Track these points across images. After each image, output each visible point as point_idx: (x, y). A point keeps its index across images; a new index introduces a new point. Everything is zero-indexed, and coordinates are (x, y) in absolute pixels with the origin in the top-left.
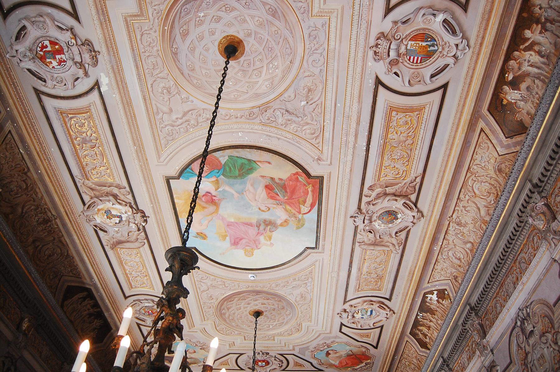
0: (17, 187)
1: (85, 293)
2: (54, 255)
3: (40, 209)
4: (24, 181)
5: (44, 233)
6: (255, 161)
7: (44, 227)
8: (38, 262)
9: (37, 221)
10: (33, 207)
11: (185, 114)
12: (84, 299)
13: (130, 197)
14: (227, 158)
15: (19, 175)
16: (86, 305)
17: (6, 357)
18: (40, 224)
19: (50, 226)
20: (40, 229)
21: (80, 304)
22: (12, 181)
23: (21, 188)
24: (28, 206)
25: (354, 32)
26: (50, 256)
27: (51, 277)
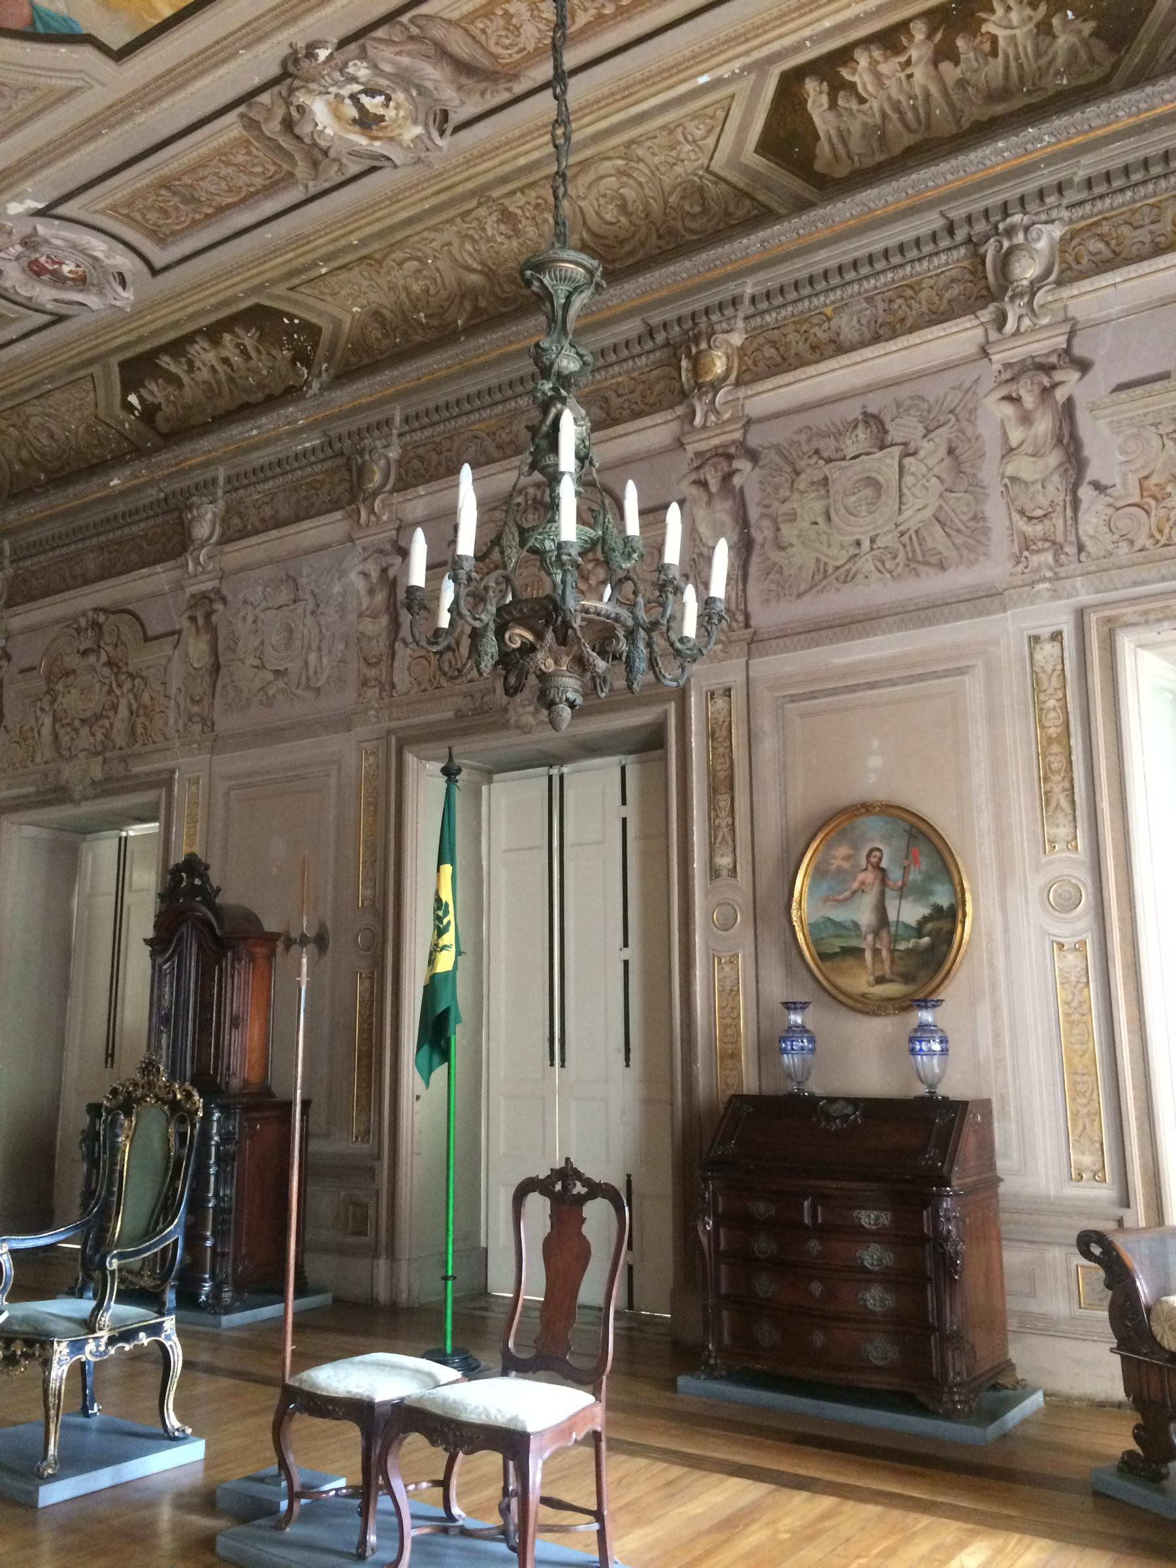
0: (416, 280)
1: (811, 85)
2: (622, 197)
3: (471, 232)
4: (400, 265)
5: (545, 221)
7: (524, 222)
8: (627, 248)
9: (508, 237)
10: (469, 247)
12: (838, 87)
13: (265, 98)
15: (388, 273)
16: (878, 76)
17: (698, 468)
18: (517, 232)
20: (532, 232)
21: (862, 101)
22: (406, 288)
23: (419, 271)
24: (467, 258)
26: (623, 208)
27: (697, 209)
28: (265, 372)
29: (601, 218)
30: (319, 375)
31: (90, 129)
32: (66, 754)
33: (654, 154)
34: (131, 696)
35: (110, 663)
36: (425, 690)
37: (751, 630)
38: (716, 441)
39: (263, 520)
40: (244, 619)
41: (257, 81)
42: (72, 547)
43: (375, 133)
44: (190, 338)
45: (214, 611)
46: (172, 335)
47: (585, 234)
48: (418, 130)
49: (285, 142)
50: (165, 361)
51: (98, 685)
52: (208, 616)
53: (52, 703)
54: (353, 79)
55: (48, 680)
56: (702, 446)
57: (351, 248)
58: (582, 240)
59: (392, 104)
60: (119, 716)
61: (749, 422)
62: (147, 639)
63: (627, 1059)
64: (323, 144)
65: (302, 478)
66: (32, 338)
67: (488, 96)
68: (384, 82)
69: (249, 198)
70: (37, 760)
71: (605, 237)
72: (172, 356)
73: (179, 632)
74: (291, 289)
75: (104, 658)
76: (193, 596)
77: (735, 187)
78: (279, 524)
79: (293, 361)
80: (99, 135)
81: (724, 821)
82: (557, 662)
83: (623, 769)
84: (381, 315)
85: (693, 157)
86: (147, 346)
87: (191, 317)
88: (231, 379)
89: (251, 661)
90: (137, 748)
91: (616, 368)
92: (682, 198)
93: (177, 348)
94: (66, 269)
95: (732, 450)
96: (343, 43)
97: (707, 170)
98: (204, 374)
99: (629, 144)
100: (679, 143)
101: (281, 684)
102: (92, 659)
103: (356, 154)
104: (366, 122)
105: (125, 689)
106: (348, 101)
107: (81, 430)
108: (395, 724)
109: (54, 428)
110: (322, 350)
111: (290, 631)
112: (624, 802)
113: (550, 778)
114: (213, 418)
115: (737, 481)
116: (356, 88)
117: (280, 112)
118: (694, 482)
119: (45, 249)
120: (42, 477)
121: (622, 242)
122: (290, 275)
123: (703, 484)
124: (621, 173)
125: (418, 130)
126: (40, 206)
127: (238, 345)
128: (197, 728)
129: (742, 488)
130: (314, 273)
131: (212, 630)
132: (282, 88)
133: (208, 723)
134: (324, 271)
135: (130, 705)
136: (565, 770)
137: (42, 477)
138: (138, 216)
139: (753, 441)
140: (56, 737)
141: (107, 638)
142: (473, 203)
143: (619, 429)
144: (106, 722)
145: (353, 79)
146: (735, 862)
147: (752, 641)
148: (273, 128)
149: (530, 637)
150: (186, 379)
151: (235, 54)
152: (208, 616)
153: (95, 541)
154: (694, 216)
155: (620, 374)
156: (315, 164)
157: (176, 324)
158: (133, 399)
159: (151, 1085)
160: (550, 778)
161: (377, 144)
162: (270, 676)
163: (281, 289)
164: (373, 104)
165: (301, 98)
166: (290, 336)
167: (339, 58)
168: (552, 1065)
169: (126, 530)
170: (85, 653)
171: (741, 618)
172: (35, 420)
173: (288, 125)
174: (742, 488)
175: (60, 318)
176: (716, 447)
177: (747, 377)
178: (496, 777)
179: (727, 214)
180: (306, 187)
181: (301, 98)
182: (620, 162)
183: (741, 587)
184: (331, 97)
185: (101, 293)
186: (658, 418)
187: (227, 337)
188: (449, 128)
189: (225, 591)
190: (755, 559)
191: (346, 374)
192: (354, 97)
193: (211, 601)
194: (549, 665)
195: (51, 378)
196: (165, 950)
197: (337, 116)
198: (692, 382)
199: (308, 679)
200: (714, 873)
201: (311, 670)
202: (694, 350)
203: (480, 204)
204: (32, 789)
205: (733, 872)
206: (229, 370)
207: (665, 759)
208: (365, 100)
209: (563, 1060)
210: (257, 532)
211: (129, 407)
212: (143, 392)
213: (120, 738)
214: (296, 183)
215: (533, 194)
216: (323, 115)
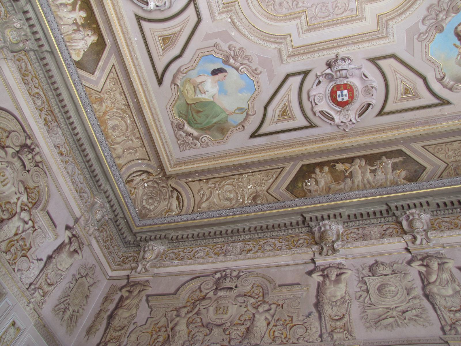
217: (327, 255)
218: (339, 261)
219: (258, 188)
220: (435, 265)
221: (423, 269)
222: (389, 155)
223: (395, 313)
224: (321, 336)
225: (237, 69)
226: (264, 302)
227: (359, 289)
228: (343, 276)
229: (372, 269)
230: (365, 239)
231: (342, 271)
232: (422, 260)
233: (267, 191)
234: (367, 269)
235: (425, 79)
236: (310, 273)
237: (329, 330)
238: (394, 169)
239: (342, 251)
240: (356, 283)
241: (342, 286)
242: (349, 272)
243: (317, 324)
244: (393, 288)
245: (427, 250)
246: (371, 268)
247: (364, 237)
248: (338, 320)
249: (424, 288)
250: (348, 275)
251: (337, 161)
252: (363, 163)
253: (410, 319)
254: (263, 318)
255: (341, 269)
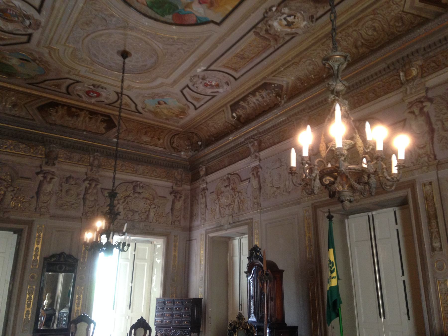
2: (374, 26)
4: (305, 62)
5: (349, 39)
6: (148, 6)
7: (342, 41)
8: (377, 42)
11: (172, 45)
13: (260, 25)
14: (167, 17)
17: (410, 107)
19: (341, 38)
20: (345, 44)
23: (310, 63)
25: (52, 34)
26: (375, 30)
28: (268, 101)
29: (367, 34)
30: (284, 99)
31: (215, 46)
32: (223, 216)
33: (383, 11)
34: (238, 198)
35: (232, 189)
36: (322, 190)
37: (437, 161)
38: (417, 97)
39: (270, 143)
40: (267, 173)
41: (257, 21)
42: (221, 158)
43: (292, 26)
44: (247, 96)
45: (259, 171)
46: (243, 95)
47: (362, 40)
48: (305, 23)
49: (267, 36)
50: (242, 103)
51: (230, 196)
52: (257, 173)
53: (219, 201)
54: (284, 13)
55: (217, 195)
56: (411, 100)
57: (289, 61)
58: (362, 43)
59: (296, 18)
60: (236, 204)
61: (427, 90)
62: (242, 181)
63: (409, 317)
64: (278, 34)
65: (281, 130)
66: (207, 103)
67: (325, 8)
68: (293, 12)
69: (258, 54)
70: (216, 218)
71: (368, 40)
72: (243, 101)
73: (250, 178)
74: (274, 76)
75: (231, 188)
76: (253, 167)
77: (413, 14)
78: (275, 144)
79: (276, 96)
80: (217, 46)
81: (434, 230)
82: (343, 187)
83: (395, 212)
84: (300, 78)
85: (397, 8)
86: (236, 100)
87: (247, 90)
88: (259, 105)
89: (270, 185)
90: (241, 213)
91: (377, 80)
92: (395, 22)
93: (244, 99)
94: (213, 83)
95: (422, 99)
96: (279, 5)
97: (403, 11)
98: (252, 105)
99: (374, 10)
100: (391, 5)
101: (279, 191)
102: (228, 188)
103: (287, 34)
104: (289, 25)
105: (237, 196)
106: (283, 20)
107: (222, 125)
108: (314, 202)
109: (215, 126)
110: (284, 92)
111: (280, 175)
112: (397, 224)
113: (369, 216)
114: (256, 116)
115: (425, 110)
116: (285, 16)
117: (264, 28)
118: (410, 112)
119: (208, 79)
120: (213, 139)
121: (375, 40)
122: (272, 73)
123: (413, 112)
124: (372, 19)
125: (305, 23)
126: (205, 68)
127: (260, 95)
128: (256, 206)
129: (428, 112)
130: (279, 71)
131: (258, 176)
132: (264, 21)
133: (259, 204)
134: (282, 69)
135: (238, 201)
136: (374, 213)
137: (213, 139)
138: (230, 66)
139: (430, 95)
140: (220, 211)
141: (232, 182)
142: (324, 40)
143: (380, 99)
144: (232, 206)
145: (284, 13)
146: (441, 245)
147: (438, 165)
148: (263, 33)
149: (332, 179)
150: (247, 107)
151: (250, 16)
152: (257, 173)
153: (227, 155)
154: (400, 27)
155: (379, 82)
156: (276, 40)
157: (243, 92)
158: (234, 115)
159: (240, 323)
160: (369, 216)
161: (293, 30)
162: (275, 189)
163: (271, 77)
164: (290, 19)
165: (270, 22)
166: (274, 89)
167: (279, 8)
168: (381, 318)
169: (235, 151)
170: (226, 186)
171: (432, 156)
172: (210, 124)
173: (267, 31)
174: (428, 112)
175: (213, 97)
176: (416, 99)
177: (425, 75)
178: (350, 217)
179: (412, 23)
180: (274, 47)
181: (270, 22)
182: (372, 16)
183: (431, 145)
184: (278, 20)
185: (223, 88)
186: (393, 93)
187: (257, 94)
188: (314, 20)
189: (261, 165)
190: (436, 135)
191: (291, 97)
192: (285, 19)
193: (258, 168)
194: (340, 188)
195: (213, 113)
196: (250, 275)
197: (281, 25)
198: (405, 80)
199: (286, 189)
200: (433, 249)
201: (287, 187)
202: (404, 69)
203: (327, 39)
204: (215, 226)
205: (441, 249)
206: (258, 102)
207: (408, 208)
208: (289, 19)
209: (384, 316)
210: (269, 147)
211: (233, 117)
212: (237, 113)
213: (236, 210)
214: (270, 47)
215: (344, 32)
216: (276, 25)
217: (49, 165)
218: (53, 170)
219: (18, 101)
220: (93, 185)
221: (88, 186)
222: (102, 115)
223: (69, 204)
224: (36, 209)
225: (38, 65)
226: (11, 186)
227: (58, 189)
228: (53, 180)
229: (68, 179)
230: (70, 160)
231: (54, 177)
232: (90, 181)
233: (24, 105)
234: (65, 178)
235: (136, 105)
236: (38, 173)
237: (40, 207)
238: (101, 121)
239: (57, 165)
240: (58, 185)
241: (51, 185)
242: (57, 178)
243: (35, 203)
244: (72, 192)
245: (94, 176)
246: (67, 178)
247: (70, 159)
248: (45, 203)
249: (84, 195)
250: (56, 180)
251: (74, 107)
252: (87, 113)
253: (74, 208)
254: (10, 195)
255: (53, 175)
